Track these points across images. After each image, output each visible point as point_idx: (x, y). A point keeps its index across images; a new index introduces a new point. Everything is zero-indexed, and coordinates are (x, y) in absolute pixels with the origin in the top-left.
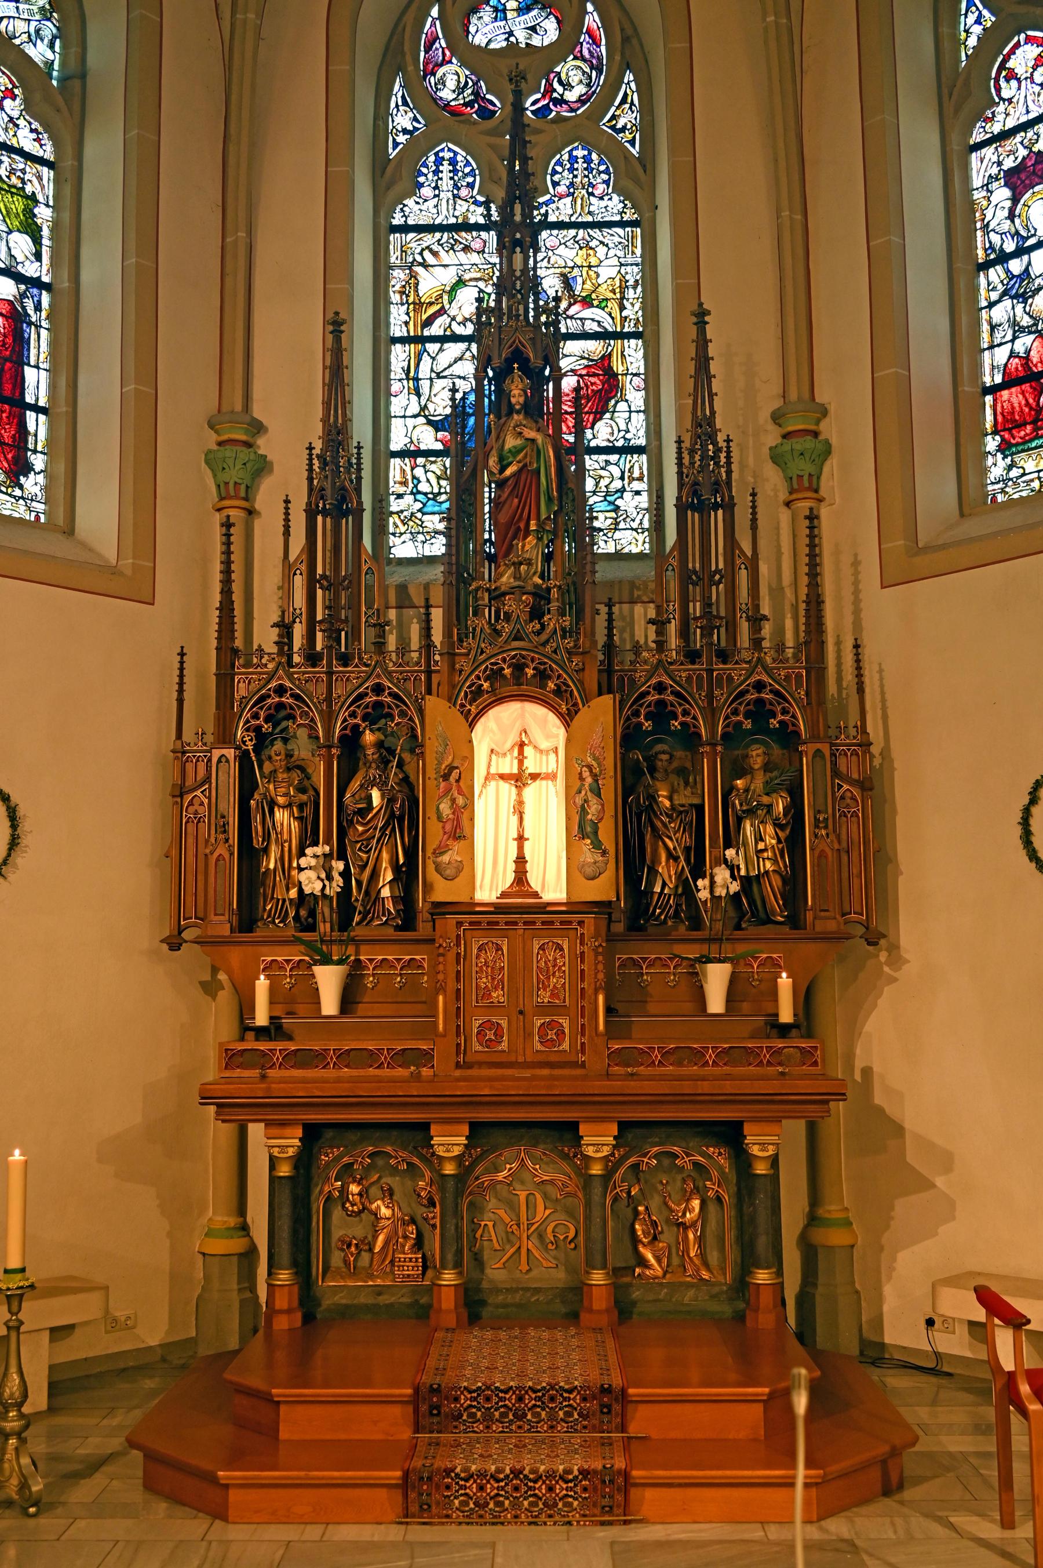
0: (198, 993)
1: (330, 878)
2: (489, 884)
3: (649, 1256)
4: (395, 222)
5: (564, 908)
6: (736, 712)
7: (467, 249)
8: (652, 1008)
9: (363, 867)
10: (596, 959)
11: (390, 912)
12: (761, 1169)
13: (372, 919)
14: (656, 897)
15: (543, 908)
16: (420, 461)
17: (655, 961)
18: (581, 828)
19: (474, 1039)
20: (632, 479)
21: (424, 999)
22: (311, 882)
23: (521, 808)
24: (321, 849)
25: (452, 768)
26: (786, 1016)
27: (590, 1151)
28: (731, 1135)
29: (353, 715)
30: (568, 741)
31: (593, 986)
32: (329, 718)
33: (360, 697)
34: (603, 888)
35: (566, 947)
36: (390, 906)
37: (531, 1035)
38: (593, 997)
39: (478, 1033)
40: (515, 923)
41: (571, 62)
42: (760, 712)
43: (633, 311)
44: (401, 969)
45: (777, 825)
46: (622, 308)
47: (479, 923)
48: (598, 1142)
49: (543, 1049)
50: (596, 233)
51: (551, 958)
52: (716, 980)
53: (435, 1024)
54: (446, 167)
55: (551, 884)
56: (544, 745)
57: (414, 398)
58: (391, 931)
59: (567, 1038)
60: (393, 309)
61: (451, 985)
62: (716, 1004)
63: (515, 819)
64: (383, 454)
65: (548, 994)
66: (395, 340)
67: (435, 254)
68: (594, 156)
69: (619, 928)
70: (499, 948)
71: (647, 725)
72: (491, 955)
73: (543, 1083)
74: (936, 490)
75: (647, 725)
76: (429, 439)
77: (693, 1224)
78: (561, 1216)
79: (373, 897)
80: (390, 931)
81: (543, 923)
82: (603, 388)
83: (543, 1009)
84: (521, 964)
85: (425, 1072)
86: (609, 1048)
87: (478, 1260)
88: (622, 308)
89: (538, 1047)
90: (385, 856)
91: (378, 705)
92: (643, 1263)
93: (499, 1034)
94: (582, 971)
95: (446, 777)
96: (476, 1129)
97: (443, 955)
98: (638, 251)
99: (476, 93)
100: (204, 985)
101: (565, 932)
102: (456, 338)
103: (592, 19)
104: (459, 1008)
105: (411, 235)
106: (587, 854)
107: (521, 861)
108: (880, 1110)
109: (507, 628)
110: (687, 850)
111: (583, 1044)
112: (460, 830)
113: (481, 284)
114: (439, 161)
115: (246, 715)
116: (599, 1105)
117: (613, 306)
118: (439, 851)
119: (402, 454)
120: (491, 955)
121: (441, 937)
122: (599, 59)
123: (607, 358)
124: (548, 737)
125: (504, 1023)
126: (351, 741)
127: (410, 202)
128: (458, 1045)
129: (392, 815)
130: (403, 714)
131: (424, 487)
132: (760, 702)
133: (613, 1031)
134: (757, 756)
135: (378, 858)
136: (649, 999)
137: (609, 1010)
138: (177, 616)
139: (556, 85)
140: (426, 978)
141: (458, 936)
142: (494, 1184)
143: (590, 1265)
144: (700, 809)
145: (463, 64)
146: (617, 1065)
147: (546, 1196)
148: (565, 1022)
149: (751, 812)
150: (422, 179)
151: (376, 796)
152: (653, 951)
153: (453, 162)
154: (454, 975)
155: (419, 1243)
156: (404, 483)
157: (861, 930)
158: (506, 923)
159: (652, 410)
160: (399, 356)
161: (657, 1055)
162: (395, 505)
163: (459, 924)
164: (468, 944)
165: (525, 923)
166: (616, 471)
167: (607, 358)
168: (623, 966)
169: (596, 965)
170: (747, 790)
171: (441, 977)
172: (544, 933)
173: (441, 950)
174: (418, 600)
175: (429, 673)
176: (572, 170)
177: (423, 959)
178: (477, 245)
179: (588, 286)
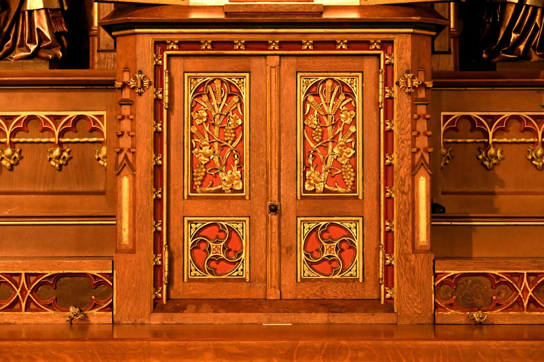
5: (354, 15)
8: (504, 203)
10: (414, 111)
11: (42, 37)
13: (11, 50)
14: (511, 10)
19: (188, 257)
21: (102, 188)
31: (407, 161)
35: (357, 90)
36: (42, 23)
37: (292, 250)
38: (408, 181)
39: (195, 247)
40: (265, 44)
44: (61, 135)
47: (197, 44)
49: (314, 275)
51: (329, 110)
53: (116, 229)
58: (44, 67)
59: (359, 257)
61: (145, 157)
65: (324, 176)
69: (448, 63)
70: (233, 92)
72: (217, 104)
73: (317, 343)
79: (14, 8)
80: (41, 70)
81: (317, 44)
83: (312, 202)
84: (275, 119)
85: (97, 317)
86: (436, 276)
89: (308, 273)
94: (389, 133)
97: (130, 103)
101: (355, 63)
104: (158, 201)
111: (388, 268)
121: (126, 69)
125: (243, 229)
128: (158, 268)
136: (497, 189)
140: (104, 150)
141: (158, 68)
146: (451, 306)
152: (504, 105)
154: (151, 139)
158: (248, 44)
161: (526, 290)
163: (160, 45)
164: (177, 82)
165: (282, 45)
168: (453, 129)
169: (414, 121)
171: (125, 142)
172: (319, 63)
173: (126, 94)
177: (100, 117)
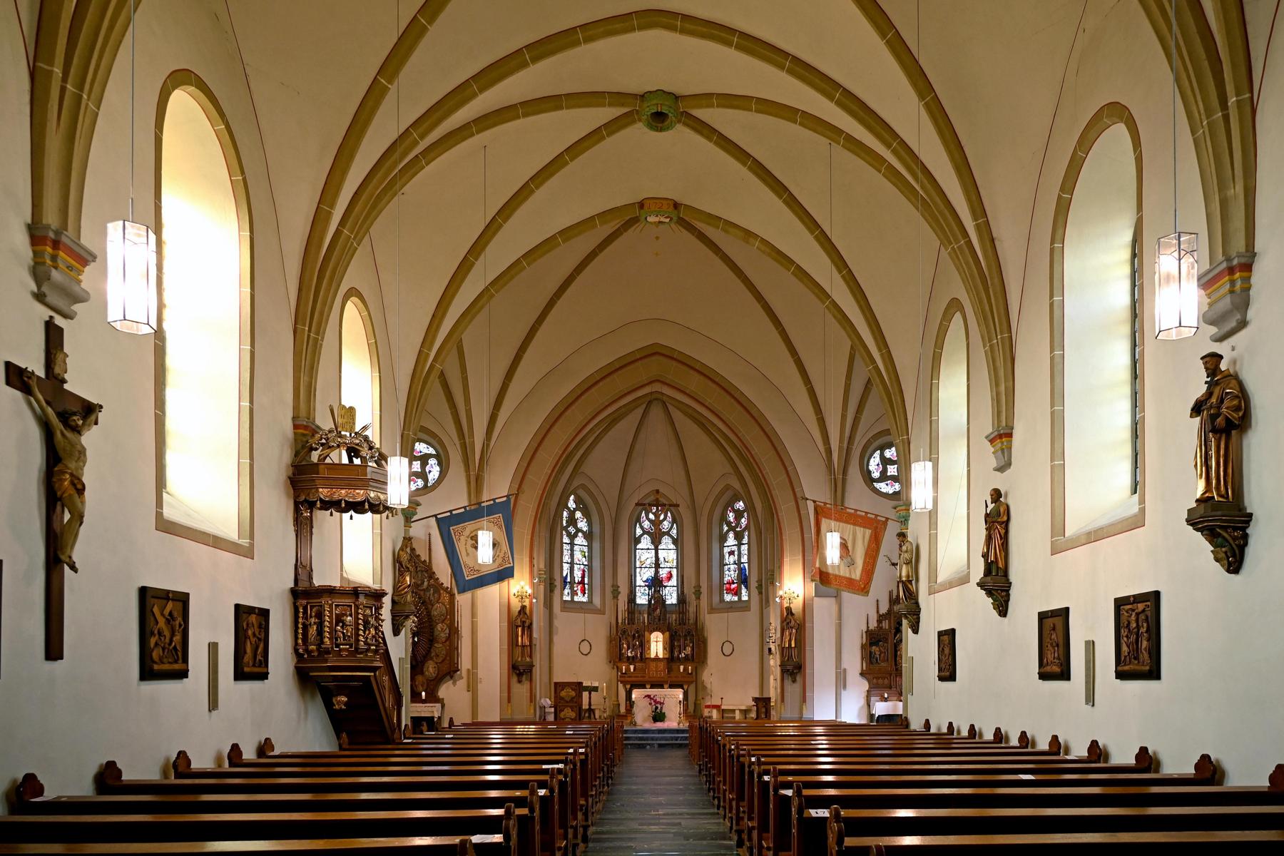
2: (653, 656)
17: (674, 666)
18: (664, 648)
23: (657, 645)
55: (661, 656)
74: (716, 599)
82: (670, 577)
138: (608, 618)
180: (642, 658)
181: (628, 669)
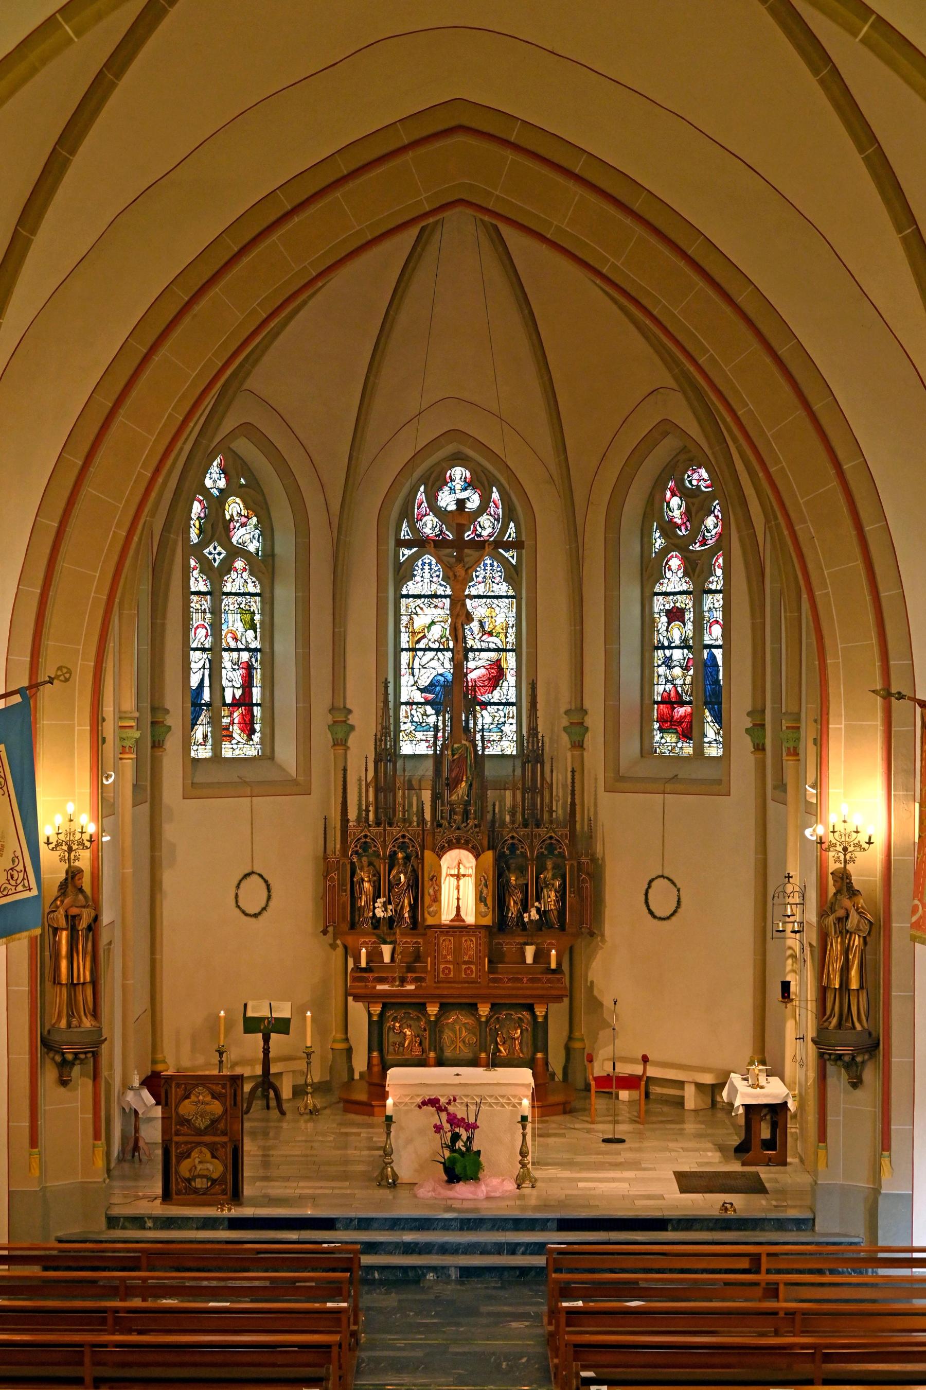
0: (328, 948)
1: (386, 910)
2: (447, 916)
3: (502, 1049)
4: (403, 593)
6: (541, 848)
7: (436, 607)
9: (397, 905)
12: (540, 1020)
15: (467, 927)
16: (414, 707)
17: (508, 944)
18: (480, 898)
20: (509, 718)
22: (379, 913)
23: (458, 888)
24: (382, 900)
25: (434, 876)
26: (553, 966)
27: (481, 1013)
28: (530, 1008)
29: (394, 846)
30: (476, 866)
32: (385, 847)
33: (397, 839)
34: (487, 921)
41: (485, 516)
42: (551, 848)
43: (511, 639)
45: (556, 891)
46: (506, 637)
48: (484, 1010)
50: (495, 601)
52: (530, 951)
54: (427, 567)
55: (470, 918)
56: (467, 865)
57: (411, 677)
60: (402, 634)
62: (529, 960)
63: (456, 892)
64: (398, 704)
66: (403, 650)
67: (422, 609)
68: (495, 563)
71: (507, 852)
72: (447, 943)
75: (507, 852)
76: (418, 697)
77: (518, 1038)
78: (471, 1035)
82: (496, 676)
87: (442, 1050)
88: (506, 637)
90: (406, 901)
91: (403, 843)
92: (500, 1051)
93: (450, 971)
95: (431, 880)
96: (442, 1006)
98: (514, 610)
99: (441, 531)
100: (331, 945)
102: (430, 649)
103: (495, 496)
105: (411, 599)
106: (483, 908)
107: (458, 908)
108: (596, 998)
109: (454, 826)
110: (522, 900)
112: (437, 899)
113: (442, 624)
114: (423, 564)
115: (352, 846)
116: (484, 998)
117: (502, 636)
118: (430, 906)
119: (406, 704)
120: (447, 943)
122: (498, 515)
123: (499, 661)
124: (469, 862)
125: (451, 967)
126: (393, 855)
127: (410, 583)
129: (409, 885)
130: (413, 846)
131: (416, 719)
132: (551, 844)
133: (492, 970)
134: (549, 864)
135: (404, 902)
137: (490, 962)
139: (478, 528)
142: (448, 1024)
143: (481, 1051)
144: (527, 885)
145: (435, 515)
147: (466, 1028)
148: (473, 967)
149: (547, 886)
150: (415, 573)
151: (402, 876)
153: (430, 565)
155: (421, 1044)
156: (407, 717)
157: (588, 931)
159: (518, 686)
160: (405, 657)
162: (403, 727)
166: (502, 714)
167: (499, 661)
170: (545, 878)
174: (416, 787)
175: (423, 830)
176: (485, 570)
178: (440, 605)
179: (491, 626)
180: (415, 916)
181: (375, 955)
